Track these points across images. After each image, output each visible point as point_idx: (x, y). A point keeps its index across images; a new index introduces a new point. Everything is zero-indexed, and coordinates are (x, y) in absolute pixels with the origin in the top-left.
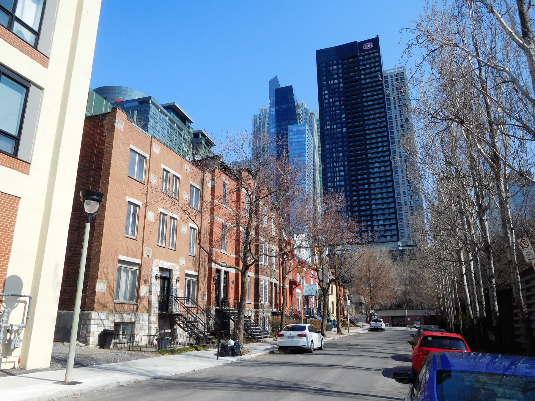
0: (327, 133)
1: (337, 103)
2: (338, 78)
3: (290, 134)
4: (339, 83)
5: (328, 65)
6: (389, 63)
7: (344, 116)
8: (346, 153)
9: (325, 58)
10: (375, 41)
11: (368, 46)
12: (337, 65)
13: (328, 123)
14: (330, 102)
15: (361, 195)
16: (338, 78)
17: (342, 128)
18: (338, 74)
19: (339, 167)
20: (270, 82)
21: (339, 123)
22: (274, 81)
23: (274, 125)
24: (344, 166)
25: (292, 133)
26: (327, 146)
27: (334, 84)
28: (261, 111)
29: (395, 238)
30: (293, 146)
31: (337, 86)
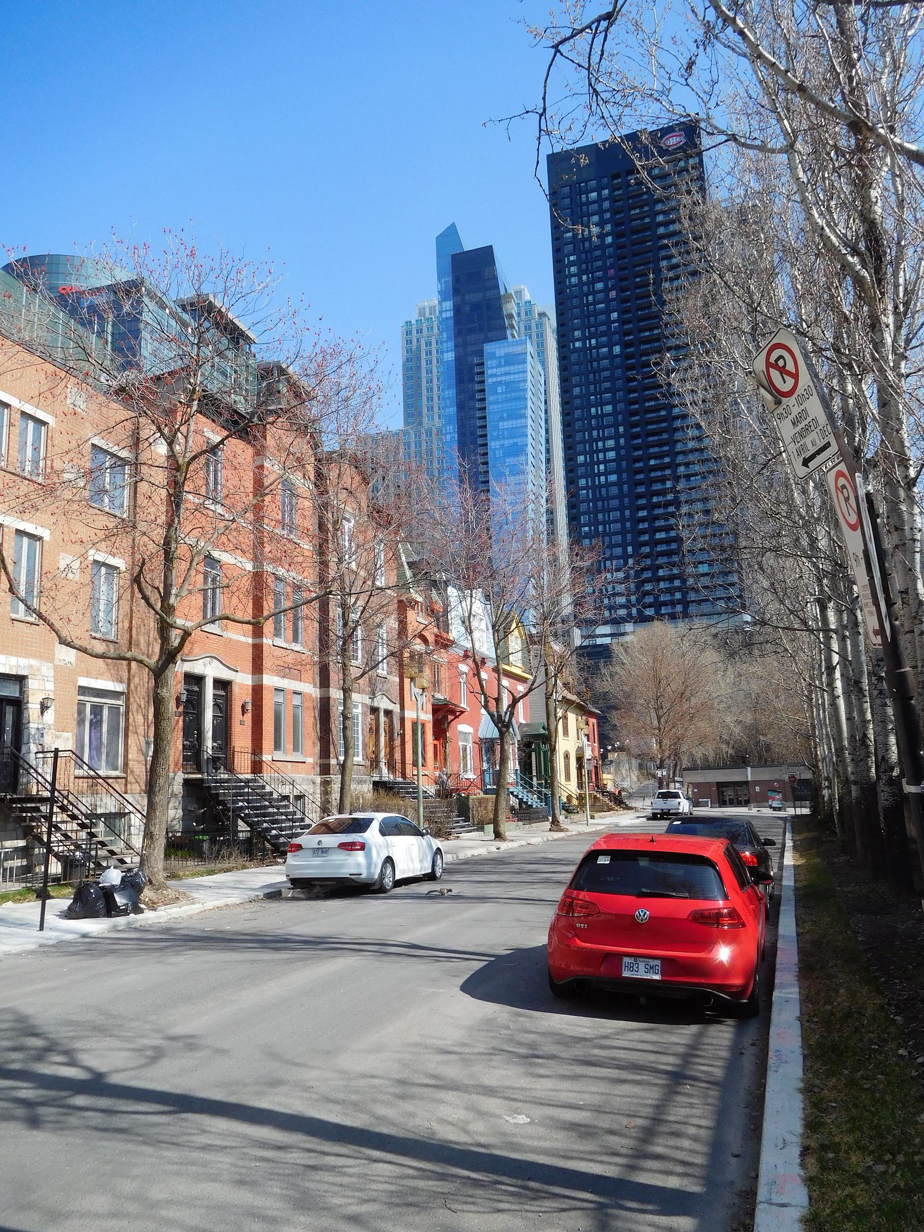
0: (574, 357)
1: (600, 286)
3: (489, 363)
5: (577, 190)
7: (614, 315)
8: (621, 406)
11: (673, 141)
12: (599, 189)
13: (577, 334)
14: (581, 283)
15: (658, 505)
16: (601, 224)
17: (610, 345)
18: (600, 212)
19: (604, 439)
20: (440, 240)
21: (603, 334)
22: (450, 235)
23: (451, 345)
24: (616, 437)
25: (494, 362)
26: (577, 391)
28: (422, 312)
30: (496, 393)
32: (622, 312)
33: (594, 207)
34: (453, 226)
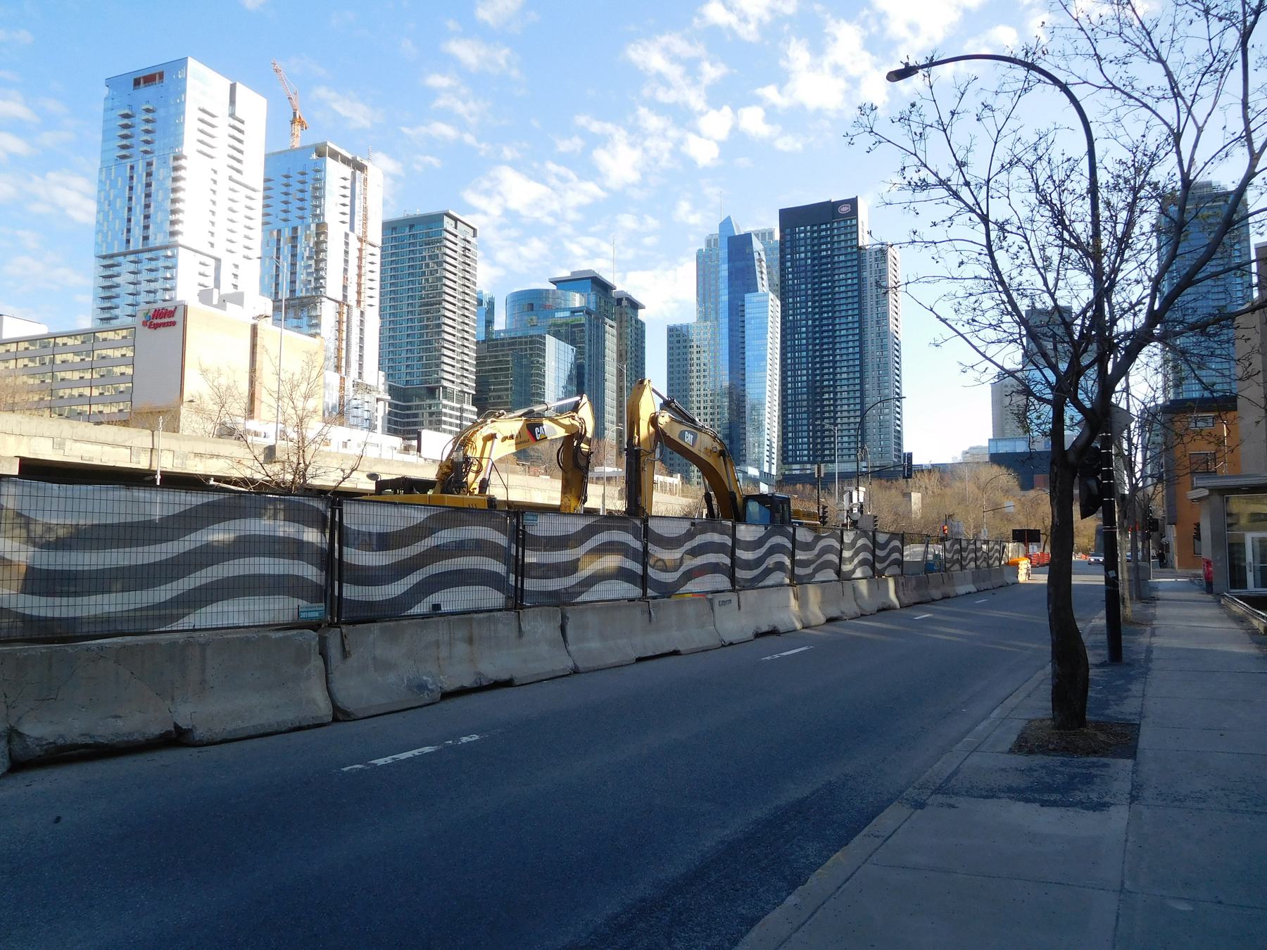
2: (806, 252)
4: (806, 258)
9: (790, 218)
10: (853, 203)
11: (845, 209)
16: (806, 252)
17: (807, 320)
18: (805, 246)
24: (807, 369)
27: (800, 259)
28: (708, 242)
31: (803, 262)
32: (814, 302)
33: (802, 242)
34: (729, 218)
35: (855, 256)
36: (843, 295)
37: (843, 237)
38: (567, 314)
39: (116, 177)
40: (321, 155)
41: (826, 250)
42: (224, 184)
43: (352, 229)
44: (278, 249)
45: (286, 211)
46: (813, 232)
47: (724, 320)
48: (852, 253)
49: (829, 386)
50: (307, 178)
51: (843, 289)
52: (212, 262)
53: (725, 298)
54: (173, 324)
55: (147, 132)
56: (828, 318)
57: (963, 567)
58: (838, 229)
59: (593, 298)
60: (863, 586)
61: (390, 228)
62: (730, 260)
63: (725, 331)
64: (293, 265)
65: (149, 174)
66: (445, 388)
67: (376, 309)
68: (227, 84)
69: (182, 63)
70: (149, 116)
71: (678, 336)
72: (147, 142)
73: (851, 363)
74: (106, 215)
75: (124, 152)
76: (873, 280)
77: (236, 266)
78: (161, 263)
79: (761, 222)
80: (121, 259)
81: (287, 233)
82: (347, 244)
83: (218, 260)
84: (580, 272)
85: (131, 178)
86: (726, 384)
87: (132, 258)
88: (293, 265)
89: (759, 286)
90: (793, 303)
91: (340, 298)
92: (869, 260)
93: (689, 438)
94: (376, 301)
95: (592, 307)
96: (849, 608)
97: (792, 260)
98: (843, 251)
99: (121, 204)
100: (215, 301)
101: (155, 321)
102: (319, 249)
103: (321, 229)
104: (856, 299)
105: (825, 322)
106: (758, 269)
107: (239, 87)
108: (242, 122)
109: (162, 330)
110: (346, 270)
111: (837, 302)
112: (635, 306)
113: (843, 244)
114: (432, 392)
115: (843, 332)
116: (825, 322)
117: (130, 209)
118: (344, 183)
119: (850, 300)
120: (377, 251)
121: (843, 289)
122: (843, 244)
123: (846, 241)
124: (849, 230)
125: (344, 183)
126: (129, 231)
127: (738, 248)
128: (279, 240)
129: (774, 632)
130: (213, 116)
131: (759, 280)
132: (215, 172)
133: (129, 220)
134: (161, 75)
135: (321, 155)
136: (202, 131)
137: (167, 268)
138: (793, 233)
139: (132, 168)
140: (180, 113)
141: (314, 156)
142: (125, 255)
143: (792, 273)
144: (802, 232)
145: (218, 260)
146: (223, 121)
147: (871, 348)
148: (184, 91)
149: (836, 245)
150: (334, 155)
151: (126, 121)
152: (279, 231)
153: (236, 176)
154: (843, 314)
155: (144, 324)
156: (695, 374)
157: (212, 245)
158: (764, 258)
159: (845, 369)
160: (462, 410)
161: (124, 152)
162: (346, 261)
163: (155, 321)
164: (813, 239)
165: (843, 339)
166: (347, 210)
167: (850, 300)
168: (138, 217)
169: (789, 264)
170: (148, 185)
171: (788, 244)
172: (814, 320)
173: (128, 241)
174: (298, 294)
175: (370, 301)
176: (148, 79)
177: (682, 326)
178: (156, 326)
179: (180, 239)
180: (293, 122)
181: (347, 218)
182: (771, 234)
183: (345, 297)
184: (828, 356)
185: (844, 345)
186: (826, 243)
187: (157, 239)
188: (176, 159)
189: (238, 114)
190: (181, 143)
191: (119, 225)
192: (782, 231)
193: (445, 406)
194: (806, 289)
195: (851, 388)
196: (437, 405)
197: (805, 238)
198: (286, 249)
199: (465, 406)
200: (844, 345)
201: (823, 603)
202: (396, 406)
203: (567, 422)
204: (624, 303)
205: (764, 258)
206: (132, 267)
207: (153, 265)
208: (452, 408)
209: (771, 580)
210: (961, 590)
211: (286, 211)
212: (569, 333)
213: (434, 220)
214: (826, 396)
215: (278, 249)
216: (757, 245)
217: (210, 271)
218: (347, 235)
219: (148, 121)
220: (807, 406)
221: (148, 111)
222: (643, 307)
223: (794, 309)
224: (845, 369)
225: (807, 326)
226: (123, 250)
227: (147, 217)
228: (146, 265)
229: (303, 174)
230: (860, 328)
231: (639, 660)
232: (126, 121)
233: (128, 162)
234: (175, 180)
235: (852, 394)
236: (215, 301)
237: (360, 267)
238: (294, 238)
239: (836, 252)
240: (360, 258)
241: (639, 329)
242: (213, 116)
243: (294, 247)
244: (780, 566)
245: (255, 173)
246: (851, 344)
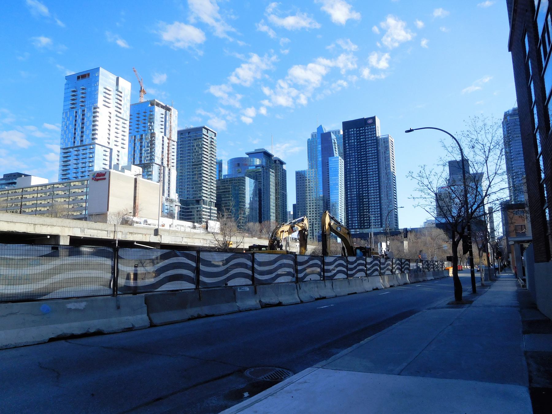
2: (354, 139)
4: (354, 142)
6: (380, 133)
9: (347, 125)
10: (374, 118)
11: (370, 121)
14: (349, 153)
16: (354, 139)
17: (355, 168)
18: (354, 137)
23: (321, 156)
24: (356, 189)
28: (312, 136)
29: (380, 226)
31: (353, 144)
32: (358, 160)
33: (353, 135)
34: (321, 126)
35: (375, 141)
36: (370, 157)
37: (370, 133)
38: (254, 167)
39: (70, 116)
40: (152, 104)
41: (363, 138)
42: (114, 118)
43: (165, 135)
44: (135, 144)
45: (138, 128)
46: (357, 131)
47: (320, 169)
48: (374, 140)
49: (366, 196)
50: (147, 114)
51: (370, 155)
52: (109, 150)
53: (320, 159)
54: (105, 179)
55: (83, 97)
56: (364, 167)
57: (429, 271)
58: (368, 129)
59: (264, 160)
60: (399, 275)
61: (180, 133)
62: (322, 144)
63: (321, 173)
64: (141, 150)
65: (83, 115)
66: (203, 200)
67: (175, 167)
68: (114, 78)
69: (97, 70)
70: (83, 91)
71: (300, 175)
72: (82, 102)
73: (375, 186)
74: (65, 132)
75: (73, 106)
76: (383, 151)
77: (119, 152)
78: (88, 151)
79: (334, 126)
80: (71, 150)
81: (138, 137)
82: (163, 141)
83: (111, 149)
84: (259, 150)
85: (76, 116)
86: (321, 195)
87: (76, 149)
88: (141, 150)
89: (335, 154)
90: (350, 161)
91: (160, 163)
92: (381, 143)
93: (339, 229)
94: (175, 164)
95: (264, 164)
96: (395, 283)
97: (348, 143)
98: (370, 139)
99: (71, 127)
100: (120, 169)
101: (97, 178)
102: (152, 143)
103: (153, 135)
104: (376, 159)
105: (363, 169)
106: (334, 147)
107: (120, 79)
108: (121, 93)
109: (100, 182)
110: (163, 152)
111: (368, 160)
112: (282, 163)
113: (370, 136)
114: (198, 202)
115: (371, 173)
116: (363, 169)
117: (75, 129)
118: (162, 116)
119: (374, 159)
120: (175, 144)
121: (370, 155)
122: (370, 136)
123: (371, 135)
124: (372, 130)
125: (162, 116)
126: (75, 138)
127: (325, 138)
128: (135, 140)
129: (377, 289)
130: (110, 91)
131: (334, 151)
132: (110, 113)
133: (75, 134)
134: (89, 75)
135: (152, 104)
136: (105, 97)
137: (90, 153)
138: (348, 132)
139: (76, 112)
140: (96, 90)
141: (150, 105)
142: (73, 148)
143: (349, 148)
144: (352, 131)
145: (111, 149)
146: (113, 93)
147: (383, 179)
148: (98, 81)
149: (367, 136)
150: (158, 105)
151: (74, 93)
152: (135, 136)
153: (119, 115)
154: (371, 165)
155: (93, 179)
156: (308, 191)
157: (109, 143)
158: (336, 142)
159: (372, 189)
160: (210, 209)
161: (73, 106)
162: (163, 148)
163: (97, 178)
164: (357, 134)
165: (371, 176)
166: (163, 127)
167: (374, 159)
168: (79, 132)
169: (347, 145)
170: (83, 119)
171: (347, 136)
172: (359, 168)
173: (74, 142)
174: (143, 162)
175: (172, 164)
176: (83, 76)
177: (302, 171)
178: (98, 180)
179: (96, 141)
180: (140, 91)
181: (163, 130)
182: (339, 132)
183: (162, 163)
184: (365, 183)
185: (372, 178)
186: (363, 136)
187: (87, 141)
188: (95, 108)
189: (120, 90)
190: (97, 102)
191: (70, 136)
192: (343, 131)
193: (204, 208)
194: (355, 155)
195: (375, 196)
196: (200, 207)
197: (354, 134)
198: (138, 144)
199: (212, 208)
200: (372, 178)
201: (389, 281)
202: (183, 208)
203: (301, 225)
204: (277, 162)
205: (336, 142)
206: (76, 153)
207: (84, 152)
208: (207, 209)
209: (374, 274)
210: (429, 278)
211: (138, 128)
212: (255, 176)
213: (200, 129)
214: (365, 200)
215: (135, 144)
216: (333, 136)
217: (108, 154)
218: (163, 137)
219: (83, 93)
220: (357, 205)
221: (83, 89)
222: (285, 164)
223: (350, 163)
224: (372, 189)
225: (355, 171)
226: (72, 146)
227: (82, 132)
228: (81, 152)
229: (145, 113)
230: (378, 171)
231: (349, 294)
232: (74, 93)
233: (75, 110)
234: (94, 117)
235: (376, 199)
236: (120, 169)
237: (168, 150)
238: (141, 139)
239: (367, 139)
240: (168, 147)
241: (284, 173)
242: (110, 91)
243: (141, 143)
244: (376, 270)
245: (126, 113)
246: (374, 178)
